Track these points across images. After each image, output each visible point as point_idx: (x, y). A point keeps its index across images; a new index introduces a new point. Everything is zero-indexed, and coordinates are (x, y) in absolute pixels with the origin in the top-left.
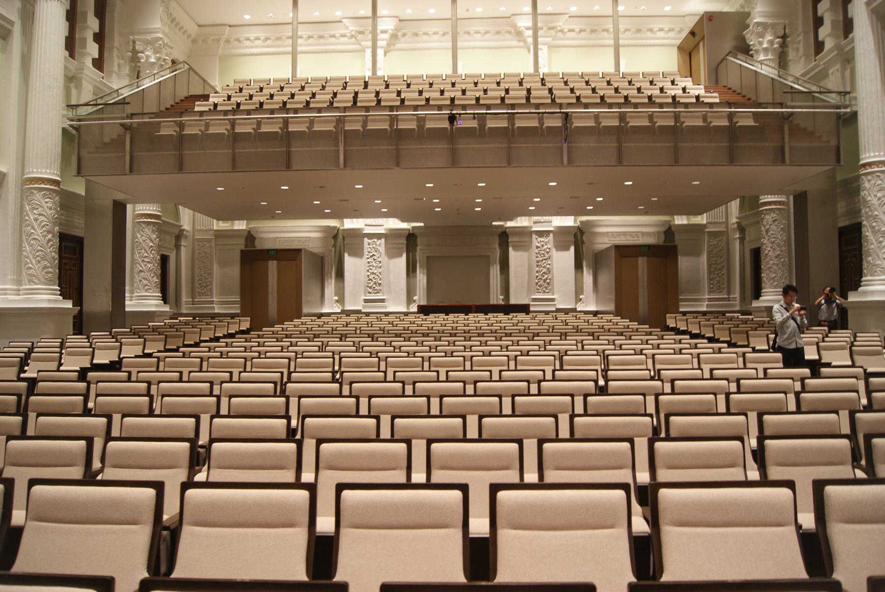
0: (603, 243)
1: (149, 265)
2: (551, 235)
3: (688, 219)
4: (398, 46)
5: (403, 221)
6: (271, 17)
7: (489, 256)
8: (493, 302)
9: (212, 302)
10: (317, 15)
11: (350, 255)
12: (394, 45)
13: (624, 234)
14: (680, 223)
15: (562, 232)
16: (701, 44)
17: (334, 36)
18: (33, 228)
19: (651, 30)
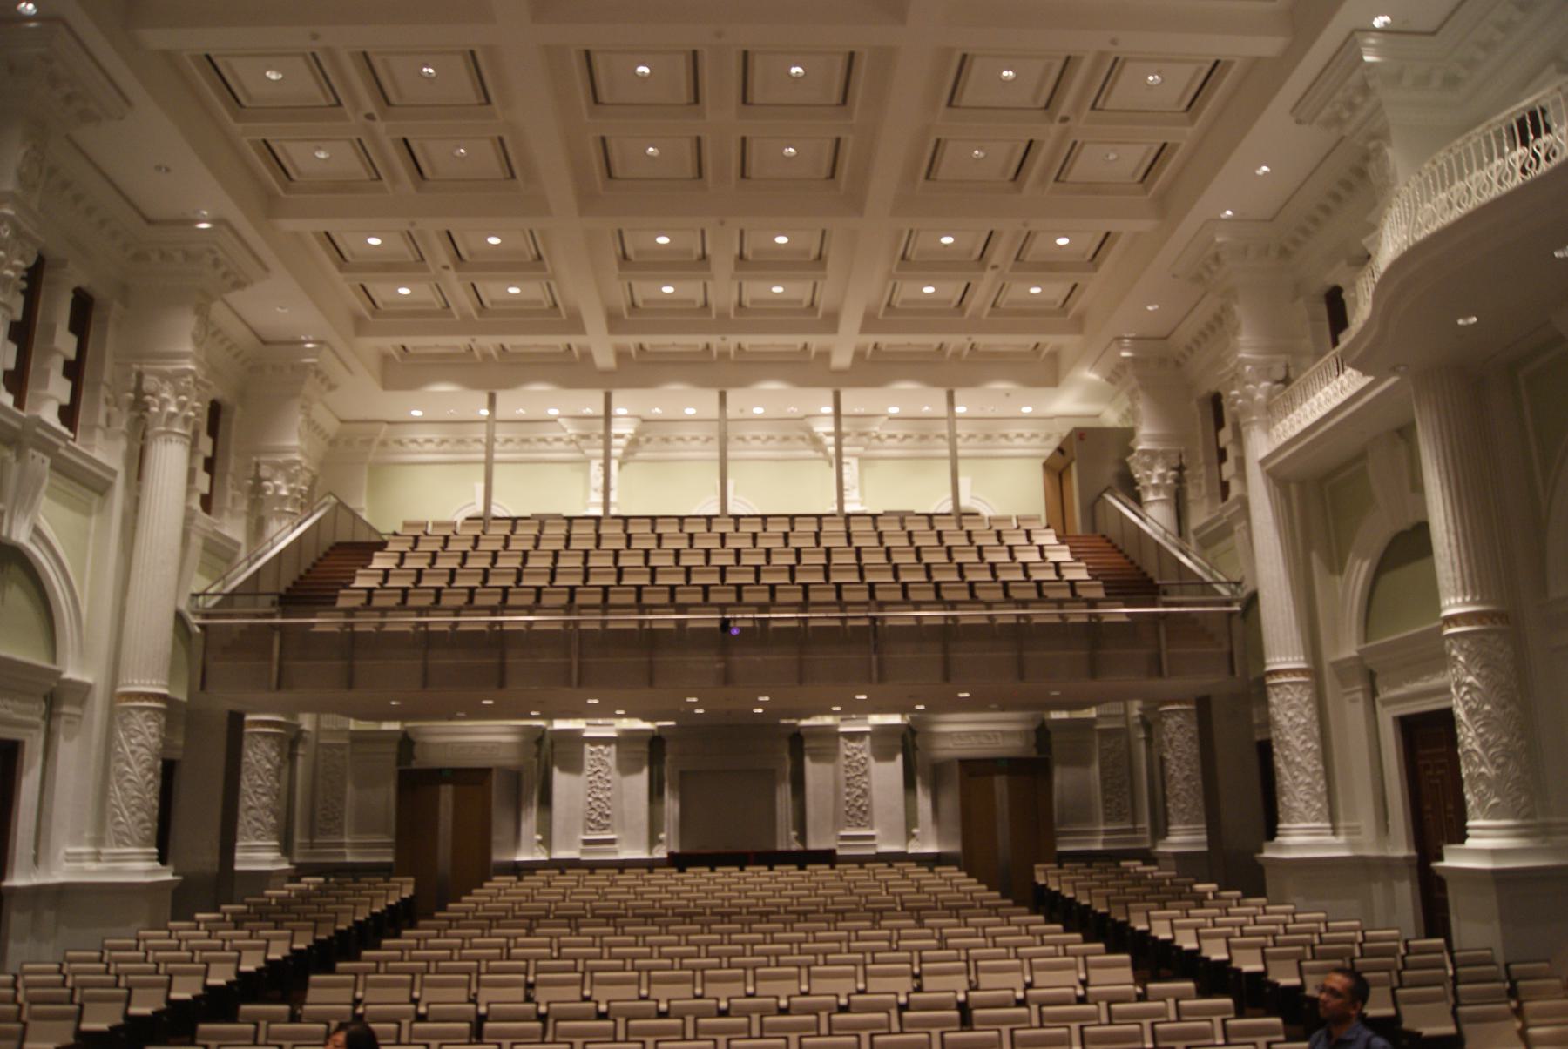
1: (264, 799)
2: (868, 738)
4: (640, 455)
5: (644, 719)
6: (452, 413)
7: (774, 771)
8: (781, 847)
9: (341, 845)
10: (521, 412)
11: (563, 769)
12: (633, 453)
13: (976, 734)
15: (882, 732)
16: (1074, 467)
17: (544, 440)
18: (129, 764)
19: (1006, 436)
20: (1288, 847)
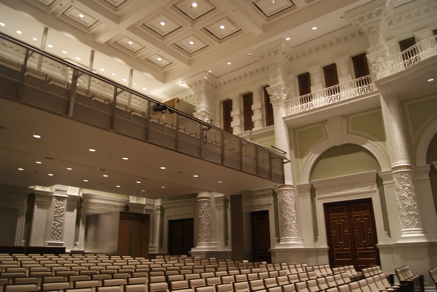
0: (93, 210)
2: (66, 200)
3: (137, 200)
13: (105, 205)
14: (133, 202)
15: (71, 198)
20: (289, 245)
